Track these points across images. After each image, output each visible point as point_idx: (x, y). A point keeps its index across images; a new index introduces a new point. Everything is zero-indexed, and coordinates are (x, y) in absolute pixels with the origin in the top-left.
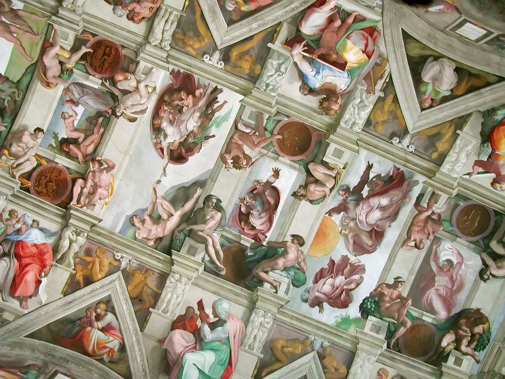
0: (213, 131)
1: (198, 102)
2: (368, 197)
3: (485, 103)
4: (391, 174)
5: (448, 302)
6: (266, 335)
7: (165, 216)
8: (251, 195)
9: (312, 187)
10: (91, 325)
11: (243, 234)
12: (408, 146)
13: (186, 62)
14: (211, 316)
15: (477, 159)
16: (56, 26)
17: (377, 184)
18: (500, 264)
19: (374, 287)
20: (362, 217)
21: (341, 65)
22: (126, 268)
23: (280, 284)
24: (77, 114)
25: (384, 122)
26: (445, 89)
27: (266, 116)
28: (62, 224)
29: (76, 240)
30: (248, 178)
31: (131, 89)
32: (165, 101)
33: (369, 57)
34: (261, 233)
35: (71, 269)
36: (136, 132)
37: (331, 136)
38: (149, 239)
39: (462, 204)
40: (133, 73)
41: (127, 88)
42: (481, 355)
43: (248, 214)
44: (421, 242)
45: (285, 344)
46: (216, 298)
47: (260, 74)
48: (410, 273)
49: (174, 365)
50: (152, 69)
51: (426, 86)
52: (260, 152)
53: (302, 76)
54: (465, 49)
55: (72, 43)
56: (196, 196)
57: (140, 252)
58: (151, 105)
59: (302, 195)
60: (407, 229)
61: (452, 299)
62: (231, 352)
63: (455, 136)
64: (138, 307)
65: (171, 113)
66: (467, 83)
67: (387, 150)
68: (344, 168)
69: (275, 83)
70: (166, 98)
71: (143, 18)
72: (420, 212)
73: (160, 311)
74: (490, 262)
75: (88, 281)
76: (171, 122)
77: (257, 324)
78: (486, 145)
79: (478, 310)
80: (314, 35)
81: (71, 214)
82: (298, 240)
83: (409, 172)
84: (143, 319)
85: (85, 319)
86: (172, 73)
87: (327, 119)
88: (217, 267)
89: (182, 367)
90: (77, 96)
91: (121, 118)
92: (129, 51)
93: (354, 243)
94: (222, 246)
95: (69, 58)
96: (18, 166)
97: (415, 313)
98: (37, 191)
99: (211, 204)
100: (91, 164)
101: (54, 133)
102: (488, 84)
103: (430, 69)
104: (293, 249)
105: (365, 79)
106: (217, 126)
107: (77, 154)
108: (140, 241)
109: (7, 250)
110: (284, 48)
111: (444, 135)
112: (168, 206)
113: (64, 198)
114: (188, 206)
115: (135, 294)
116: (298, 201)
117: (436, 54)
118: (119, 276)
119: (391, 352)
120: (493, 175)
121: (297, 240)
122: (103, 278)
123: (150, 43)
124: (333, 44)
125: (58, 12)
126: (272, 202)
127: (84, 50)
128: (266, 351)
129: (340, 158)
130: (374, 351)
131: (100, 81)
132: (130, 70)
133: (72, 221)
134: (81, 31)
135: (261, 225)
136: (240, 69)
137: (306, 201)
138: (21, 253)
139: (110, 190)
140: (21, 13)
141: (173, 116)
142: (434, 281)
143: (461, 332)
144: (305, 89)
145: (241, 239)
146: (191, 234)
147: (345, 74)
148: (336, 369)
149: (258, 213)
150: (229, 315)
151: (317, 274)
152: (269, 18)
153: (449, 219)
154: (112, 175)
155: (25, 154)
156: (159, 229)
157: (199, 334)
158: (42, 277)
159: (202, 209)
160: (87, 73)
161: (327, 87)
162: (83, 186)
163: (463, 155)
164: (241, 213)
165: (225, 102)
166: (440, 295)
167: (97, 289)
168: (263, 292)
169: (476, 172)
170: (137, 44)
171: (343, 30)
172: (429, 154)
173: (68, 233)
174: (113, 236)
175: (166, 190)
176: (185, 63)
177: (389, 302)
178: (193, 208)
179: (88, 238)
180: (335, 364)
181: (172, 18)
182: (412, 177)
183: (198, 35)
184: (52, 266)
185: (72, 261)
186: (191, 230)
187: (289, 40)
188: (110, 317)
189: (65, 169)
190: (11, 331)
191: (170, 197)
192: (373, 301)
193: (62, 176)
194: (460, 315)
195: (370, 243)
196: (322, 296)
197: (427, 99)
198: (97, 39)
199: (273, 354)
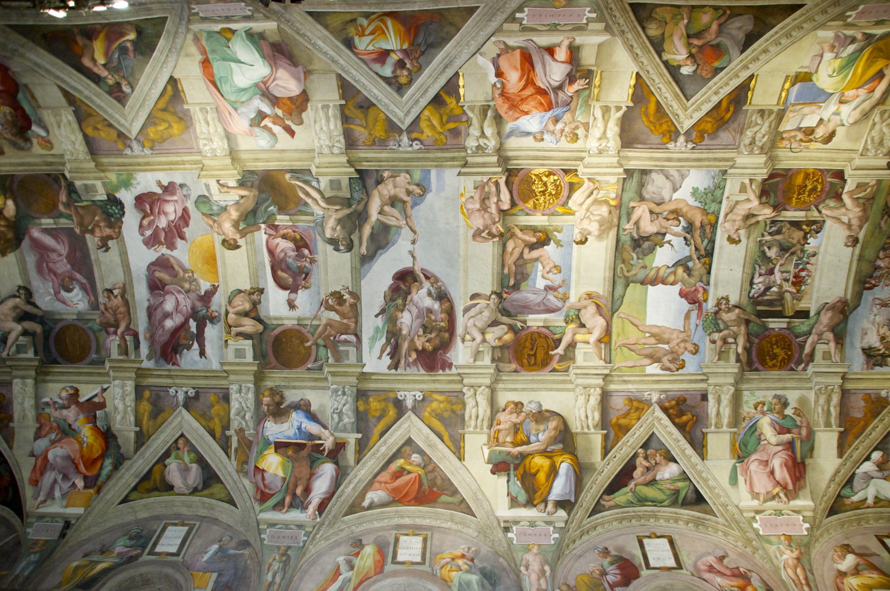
0: (380, 321)
1: (409, 346)
2: (186, 322)
3: (127, 470)
6: (198, 131)
7: (387, 209)
8: (305, 270)
10: (405, 52)
14: (270, 125)
15: (106, 409)
16: (602, 363)
17: (185, 338)
18: (18, 311)
20: (181, 297)
21: (280, 447)
22: (399, 136)
23: (221, 192)
24: (543, 277)
25: (212, 406)
26: (173, 465)
27: (331, 361)
28: (505, 150)
31: (490, 329)
33: (256, 467)
35: (467, 105)
37: (255, 368)
38: (391, 177)
40: (494, 348)
41: (495, 329)
43: (298, 248)
44: (109, 297)
45: (170, 131)
46: (279, 146)
47: (357, 401)
50: (475, 360)
52: (320, 319)
53: (313, 417)
54: (175, 509)
55: (577, 351)
56: (365, 245)
58: (461, 321)
59: (253, 293)
63: (138, 423)
64: (359, 99)
66: (155, 481)
68: (226, 341)
70: (447, 335)
71: (504, 410)
72: (128, 328)
74: (29, 308)
75: (437, 101)
76: (430, 311)
77: (216, 139)
81: (499, 166)
85: (417, 56)
86: (450, 366)
88: (298, 179)
89: (263, 57)
90: (551, 297)
91: (488, 293)
94: (306, 204)
95: (575, 334)
96: (592, 193)
97: (64, 222)
101: (562, 246)
102: (135, 489)
105: (251, 442)
108: (401, 171)
109: (560, 94)
110: (342, 439)
111: (149, 420)
112: (391, 222)
113: (516, 180)
114: (367, 230)
115: (372, 111)
118: (403, 123)
120: (82, 399)
123: (487, 387)
125: (604, 379)
126: (280, 273)
127: (560, 350)
128: (185, 114)
130: (74, 165)
131: (529, 324)
132: (498, 350)
133: (495, 159)
134: (571, 369)
135: (278, 244)
138: (539, 97)
140: (648, 361)
141: (430, 318)
142: (69, 262)
145: (291, 220)
146: (347, 202)
147: (271, 439)
148: (96, 128)
151: (189, 218)
152: (372, 462)
153: (97, 334)
154: (472, 228)
155: (588, 210)
156: (385, 192)
157: (271, 101)
159: (350, 235)
160: (547, 327)
164: (307, 246)
165: (380, 358)
166: (54, 251)
167: (421, 97)
168: (233, 176)
169: (100, 394)
171: (291, 486)
173: (492, 143)
175: (401, 237)
176: (441, 381)
177: (98, 221)
178: (360, 231)
179: (465, 149)
180: (103, 134)
181: (473, 423)
182: (156, 362)
183: (440, 417)
184: (493, 99)
185: (470, 114)
186: (350, 206)
188: (387, 71)
190: (498, 10)
191: (393, 230)
196: (168, 198)
198: (550, 368)
199: (174, 114)
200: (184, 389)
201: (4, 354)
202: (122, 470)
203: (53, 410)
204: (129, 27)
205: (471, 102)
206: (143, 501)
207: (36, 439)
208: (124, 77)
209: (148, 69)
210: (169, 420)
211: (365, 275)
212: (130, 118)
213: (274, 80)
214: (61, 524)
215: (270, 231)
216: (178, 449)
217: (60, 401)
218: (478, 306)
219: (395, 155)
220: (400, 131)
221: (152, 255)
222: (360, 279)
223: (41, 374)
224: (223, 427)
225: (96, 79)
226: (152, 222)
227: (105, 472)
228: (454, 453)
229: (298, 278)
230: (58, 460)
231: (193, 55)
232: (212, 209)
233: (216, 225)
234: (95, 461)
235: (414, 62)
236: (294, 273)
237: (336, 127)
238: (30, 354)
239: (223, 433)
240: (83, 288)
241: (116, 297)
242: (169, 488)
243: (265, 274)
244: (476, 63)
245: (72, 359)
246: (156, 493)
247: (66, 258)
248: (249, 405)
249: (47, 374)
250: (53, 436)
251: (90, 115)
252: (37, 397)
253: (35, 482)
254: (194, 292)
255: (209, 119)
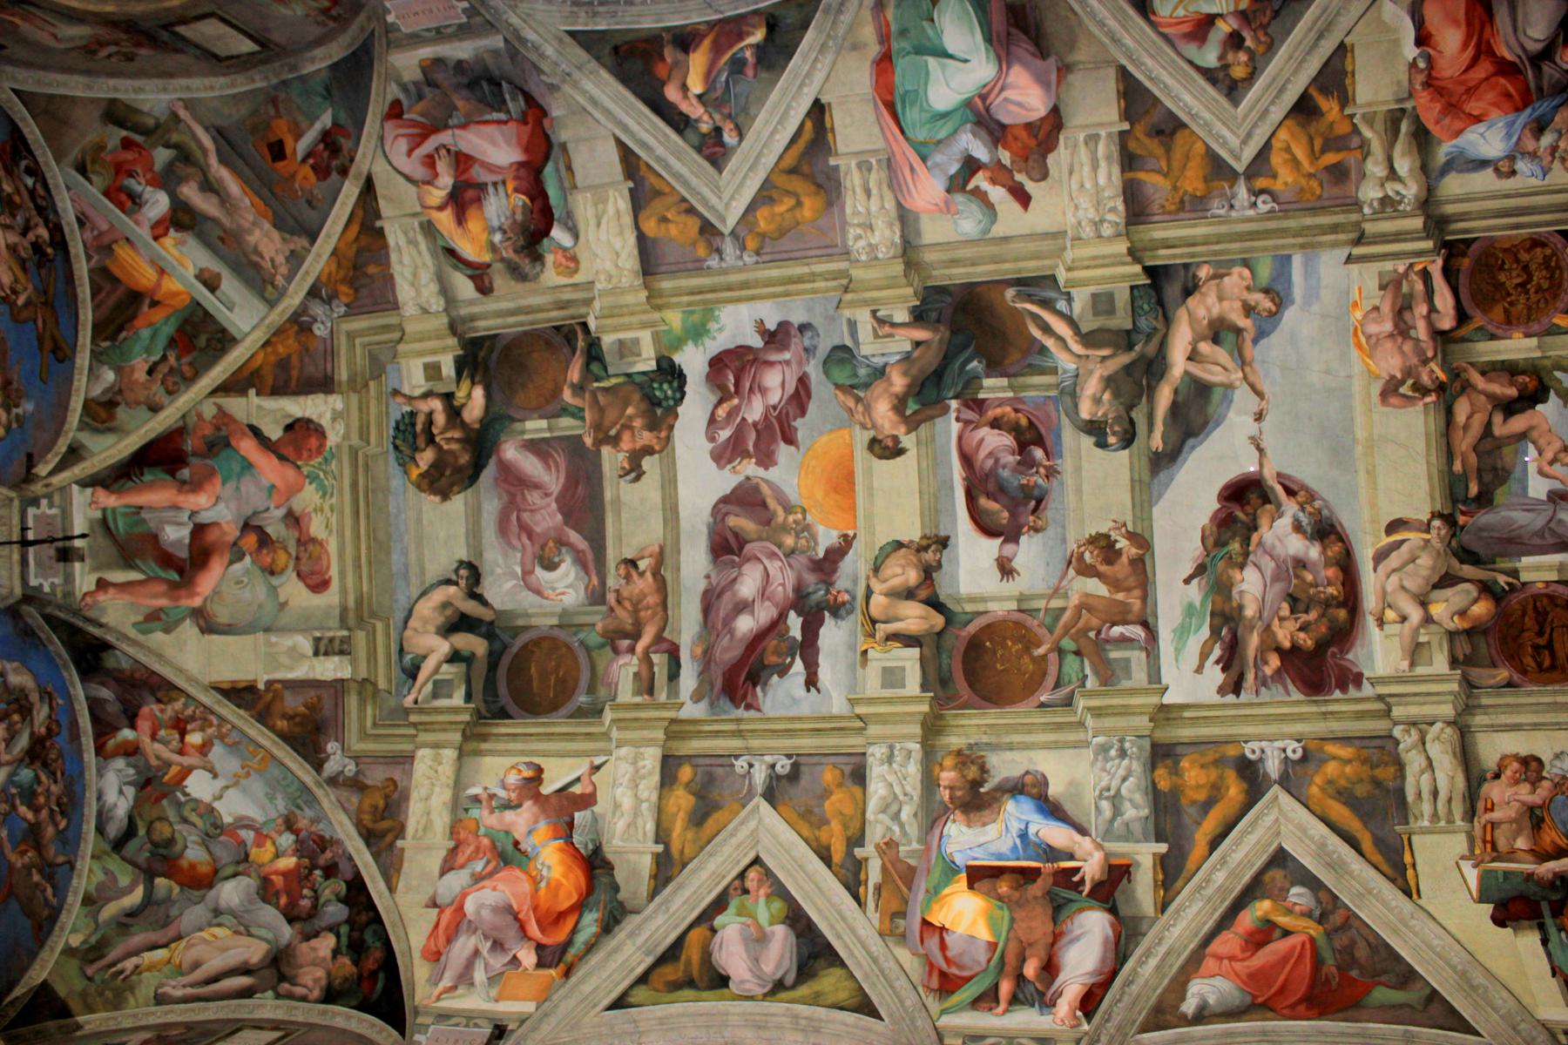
0: (1194, 592)
1: (1262, 642)
2: (782, 616)
3: (631, 935)
4: (758, 689)
5: (514, 481)
6: (848, 211)
7: (1205, 347)
8: (1036, 493)
9: (912, 577)
10: (1243, 15)
11: (1010, 399)
12: (751, 766)
13: (1339, 719)
15: (596, 809)
17: (777, 653)
18: (449, 612)
19: (677, 432)
20: (774, 567)
21: (978, 876)
22: (1231, 187)
23: (876, 336)
24: (1541, 472)
25: (826, 794)
26: (730, 926)
27: (1091, 683)
28: (1440, 203)
29: (1382, 185)
30: (1064, 527)
31: (1437, 594)
32: (1340, 605)
33: (926, 923)
34: (971, 422)
35: (1359, 112)
36: (1373, 505)
37: (925, 708)
39: (582, 699)
40: (1452, 635)
41: (1448, 592)
42: (399, 408)
43: (1022, 447)
44: (628, 577)
45: (797, 213)
46: (998, 230)
47: (1153, 768)
48: (617, 501)
49: (1009, 34)
50: (1412, 664)
51: (772, 916)
52: (1066, 596)
53: (1053, 810)
57: (1219, 239)
58: (1370, 582)
59: (926, 548)
60: (669, 589)
61: (508, 492)
62: (903, 132)
63: (661, 836)
64: (1156, 117)
65: (1311, 585)
66: (689, 962)
67: (792, 737)
68: (865, 652)
69: (1108, 766)
70: (1342, 614)
71: (1497, 776)
72: (659, 639)
73: (1103, 133)
74: (470, 607)
75: (1304, 109)
76: (1301, 564)
77: (880, 224)
78: (591, 847)
79: (445, 496)
80: (1071, 917)
81: (1428, 237)
82: (887, 449)
83: (725, 712)
84: (1134, 96)
85: (1265, 20)
86: (1358, 679)
87: (955, 741)
89: (988, 40)
91: (1425, 517)
92: (1492, 682)
93: (764, 505)
94: (1043, 350)
97: (567, 425)
98: (1543, 245)
99: (1117, 428)
100: (1442, 376)
102: (643, 979)
103: (782, 957)
104: (887, 425)
105: (912, 870)
106: (1190, 606)
107: (1490, 380)
108: (1232, 263)
110: (1123, 855)
111: (686, 829)
112: (1213, 375)
113: (1466, 263)
114: (1164, 396)
115: (1180, 137)
116: (928, 532)
117: (784, 995)
118: (1238, 158)
119: (573, 318)
120: (547, 789)
121: (887, 447)
122: (1273, 134)
123: (1449, 723)
124: (1019, 914)
126: (984, 502)
128: (829, 178)
129: (885, 669)
130: (608, 301)
131: (1524, 577)
132: (1463, 638)
133: (1417, 223)
135: (982, 440)
136: (1203, 760)
137: (911, 542)
139: (1363, 340)
141: (1303, 580)
142: (560, 509)
143: (457, 434)
144: (1034, 786)
145: (1011, 387)
146: (1125, 340)
147: (960, 860)
148: (664, 220)
149: (1003, 461)
150: (948, 209)
151: (809, 396)
152: (1195, 908)
153: (594, 654)
156: (1201, 312)
157: (991, 133)
158: (1420, 55)
159: (1130, 408)
161: (986, 812)
162: (1434, 316)
163: (627, 802)
164: (1040, 441)
165: (1199, 669)
166: (537, 486)
167: (1273, 103)
168: (904, 299)
170: (1480, 706)
171: (1011, 960)
172: (700, 770)
173: (1411, 190)
174: (1301, 240)
175: (1234, 405)
177: (631, 418)
179: (1357, 205)
180: (673, 230)
182: (712, 704)
183: (1345, 796)
184: (1411, 95)
185: (1367, 133)
186: (1130, 347)
187: (1125, 881)
189: (1499, 332)
191: (1217, 395)
192: (664, 404)
193: (1498, 312)
194: (477, 467)
195: (732, 521)
196: (774, 357)
197: (759, 888)
199: (810, 178)
200: (768, 759)
201: (408, 701)
202: (621, 934)
203: (486, 812)
204: (756, 20)
205: (1370, 105)
206: (659, 1011)
207: (443, 872)
208: (729, 116)
209: (774, 96)
210: (731, 827)
211: (1160, 496)
212: (726, 196)
213: (1002, 89)
214: (487, 1030)
215: (969, 415)
216: (746, 891)
217: (502, 793)
218: (1405, 548)
219: (1223, 229)
220: (1232, 176)
221: (725, 481)
222: (1151, 505)
223: (473, 738)
224: (848, 839)
225: (679, 122)
226: (737, 409)
227: (581, 939)
228: (1393, 881)
229: (1021, 509)
230: (486, 914)
231: (866, 45)
232: (855, 375)
233: (860, 408)
234: (561, 916)
235: (1260, 34)
236: (1013, 499)
237: (1109, 178)
238: (458, 699)
239: (849, 853)
240: (580, 561)
241: (642, 574)
242: (721, 981)
243: (954, 505)
244: (1380, 20)
245: (533, 706)
246: (688, 993)
247: (557, 501)
248: (908, 789)
249: (484, 738)
250: (479, 866)
251: (658, 194)
252: (458, 785)
253: (434, 957)
254: (802, 552)
255: (871, 185)
